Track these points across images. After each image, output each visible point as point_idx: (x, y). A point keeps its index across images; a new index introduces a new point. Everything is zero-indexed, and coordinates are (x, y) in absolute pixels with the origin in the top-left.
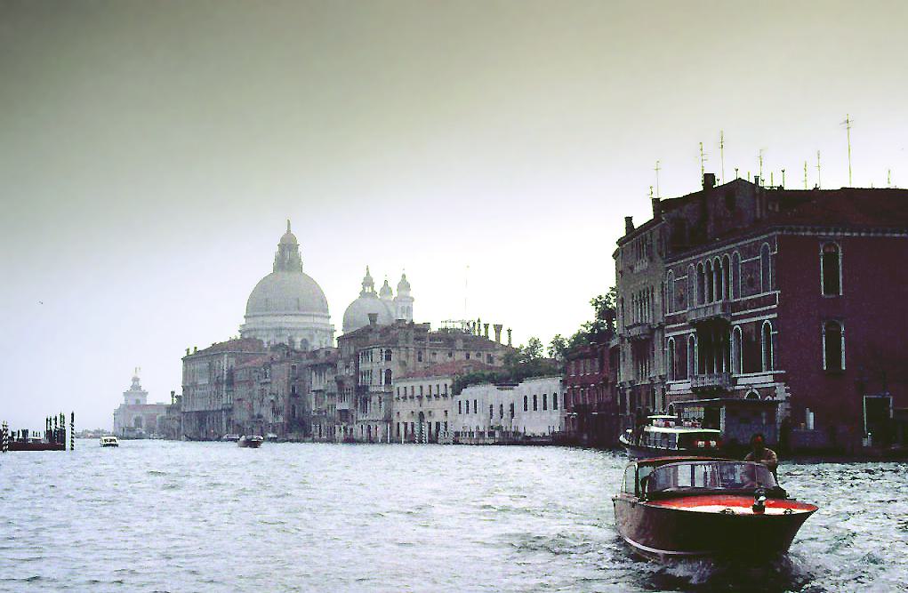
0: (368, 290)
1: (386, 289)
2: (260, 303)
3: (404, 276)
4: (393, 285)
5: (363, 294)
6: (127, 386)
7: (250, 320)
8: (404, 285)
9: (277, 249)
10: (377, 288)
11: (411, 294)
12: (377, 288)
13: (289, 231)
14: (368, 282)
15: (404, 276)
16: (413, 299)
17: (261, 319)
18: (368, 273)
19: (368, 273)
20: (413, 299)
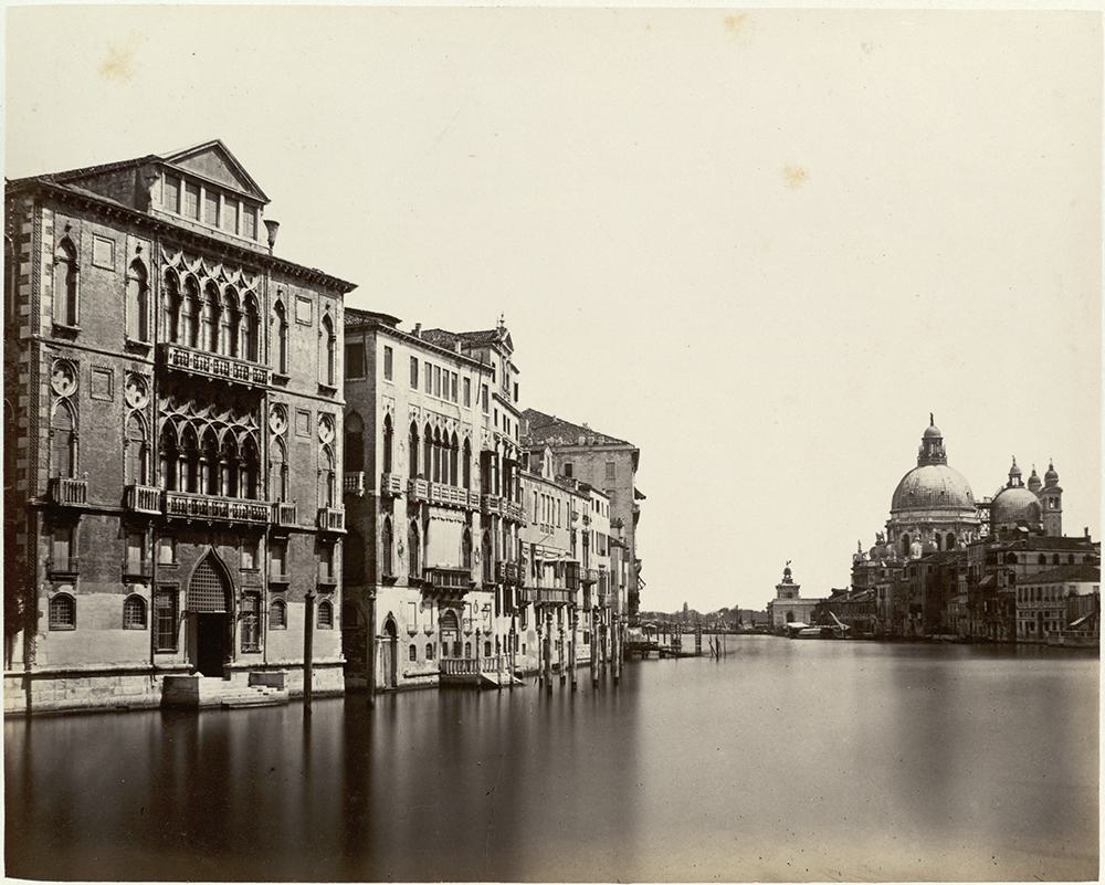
0: (1015, 481)
1: (1033, 481)
2: (907, 498)
3: (1051, 467)
4: (1041, 476)
5: (1010, 485)
6: (779, 579)
7: (896, 516)
8: (1051, 477)
9: (921, 443)
10: (1025, 479)
11: (1059, 485)
12: (1025, 479)
13: (932, 424)
14: (1014, 473)
15: (1051, 467)
16: (1060, 491)
17: (904, 515)
18: (1014, 465)
19: (1014, 465)
20: (1060, 491)
